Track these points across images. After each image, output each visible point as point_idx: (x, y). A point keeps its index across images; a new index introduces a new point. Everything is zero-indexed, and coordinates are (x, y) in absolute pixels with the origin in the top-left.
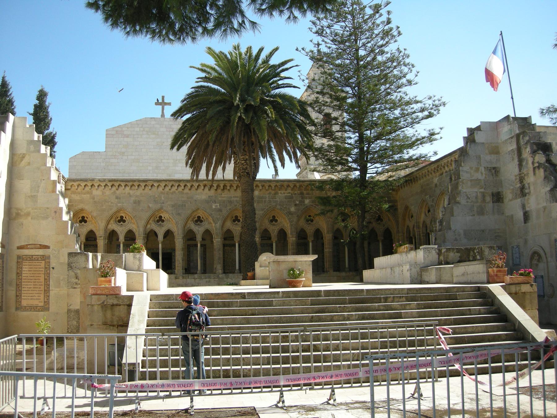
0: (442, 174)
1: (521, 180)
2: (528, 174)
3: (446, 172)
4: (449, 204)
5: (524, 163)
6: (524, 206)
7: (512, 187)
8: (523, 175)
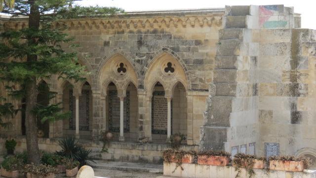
0: (123, 32)
1: (294, 78)
2: (307, 75)
3: (131, 32)
4: (216, 95)
5: (301, 63)
6: (293, 106)
7: (275, 82)
8: (298, 74)
